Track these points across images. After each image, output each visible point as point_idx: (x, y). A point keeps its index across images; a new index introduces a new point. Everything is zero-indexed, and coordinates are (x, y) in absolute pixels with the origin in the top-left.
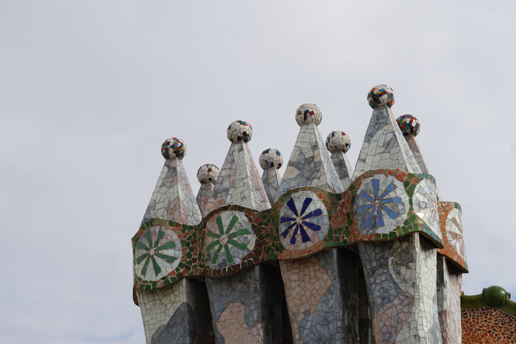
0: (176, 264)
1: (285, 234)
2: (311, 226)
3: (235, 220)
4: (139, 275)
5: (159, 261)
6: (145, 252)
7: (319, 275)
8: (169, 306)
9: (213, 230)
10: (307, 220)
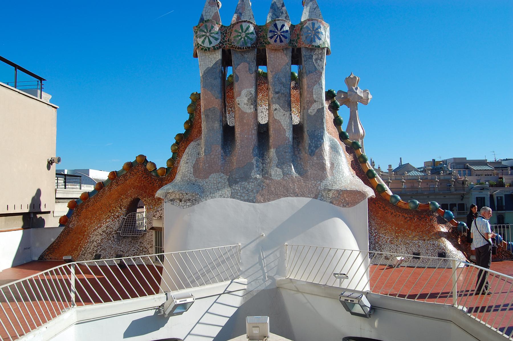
0: (219, 41)
1: (271, 38)
2: (283, 36)
3: (249, 27)
4: (200, 43)
5: (211, 39)
6: (204, 34)
7: (283, 57)
8: (213, 59)
9: (238, 29)
10: (282, 34)
